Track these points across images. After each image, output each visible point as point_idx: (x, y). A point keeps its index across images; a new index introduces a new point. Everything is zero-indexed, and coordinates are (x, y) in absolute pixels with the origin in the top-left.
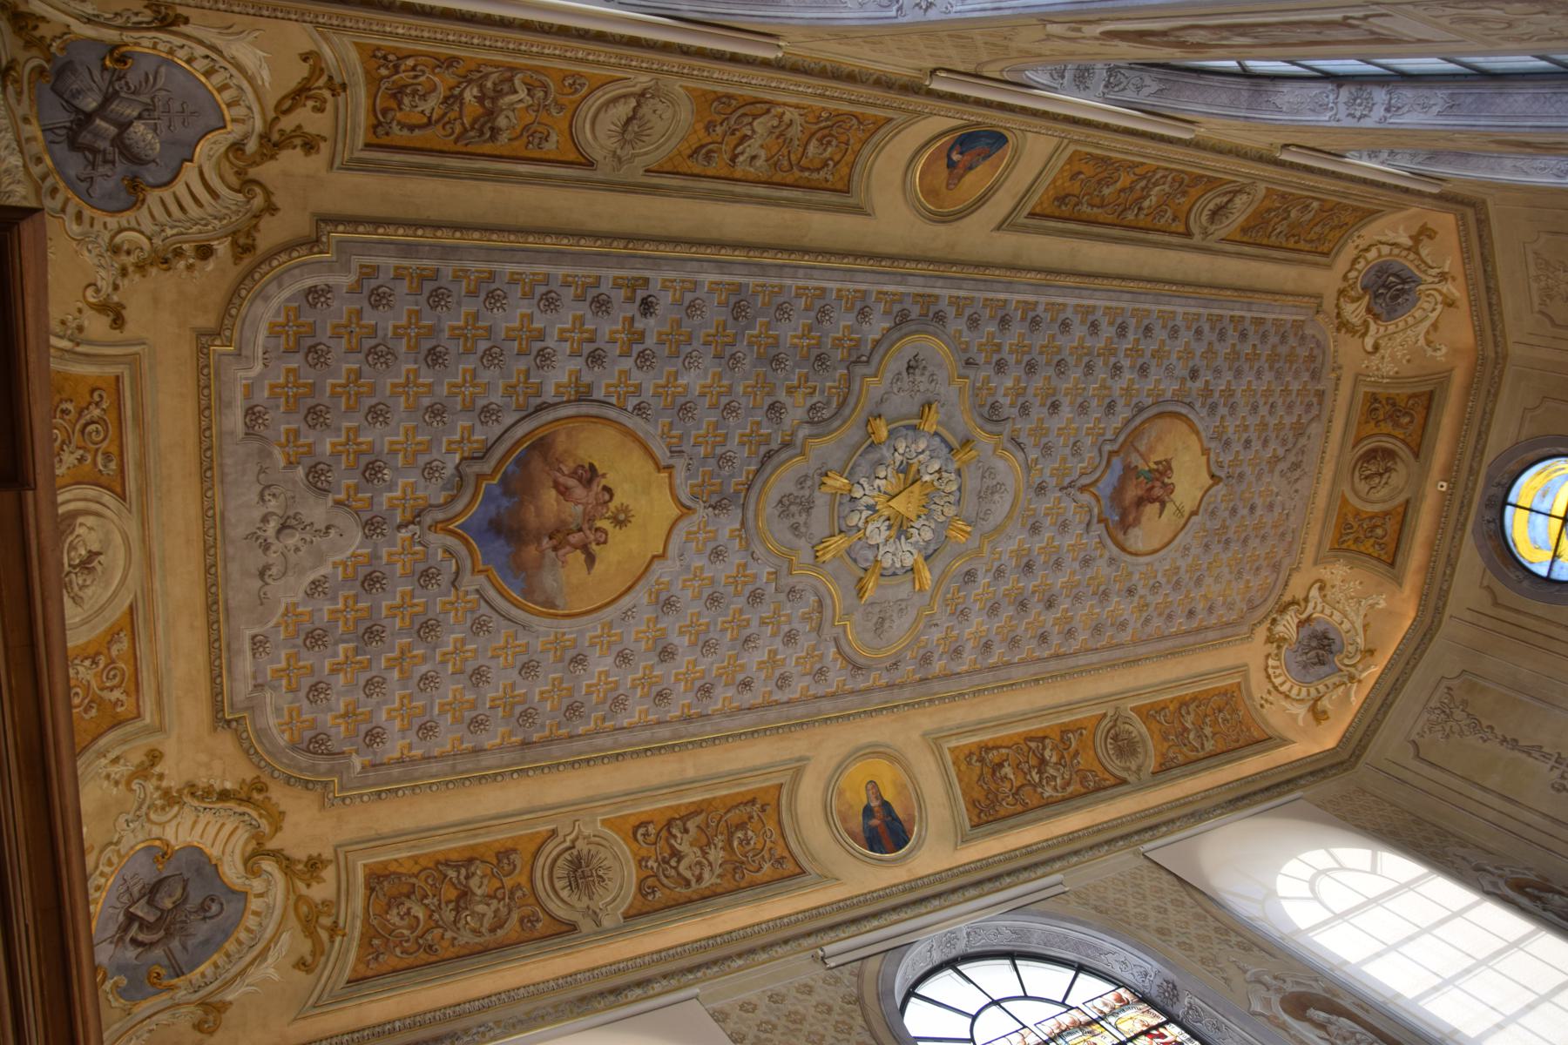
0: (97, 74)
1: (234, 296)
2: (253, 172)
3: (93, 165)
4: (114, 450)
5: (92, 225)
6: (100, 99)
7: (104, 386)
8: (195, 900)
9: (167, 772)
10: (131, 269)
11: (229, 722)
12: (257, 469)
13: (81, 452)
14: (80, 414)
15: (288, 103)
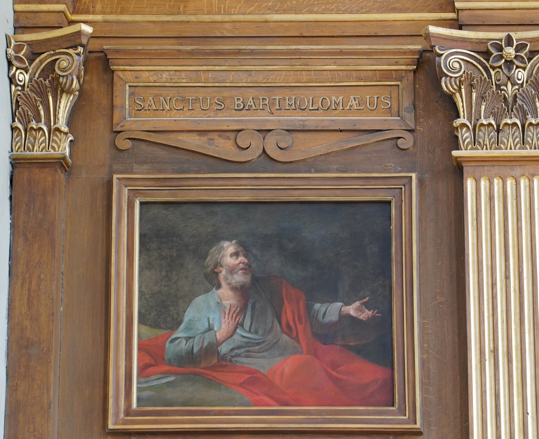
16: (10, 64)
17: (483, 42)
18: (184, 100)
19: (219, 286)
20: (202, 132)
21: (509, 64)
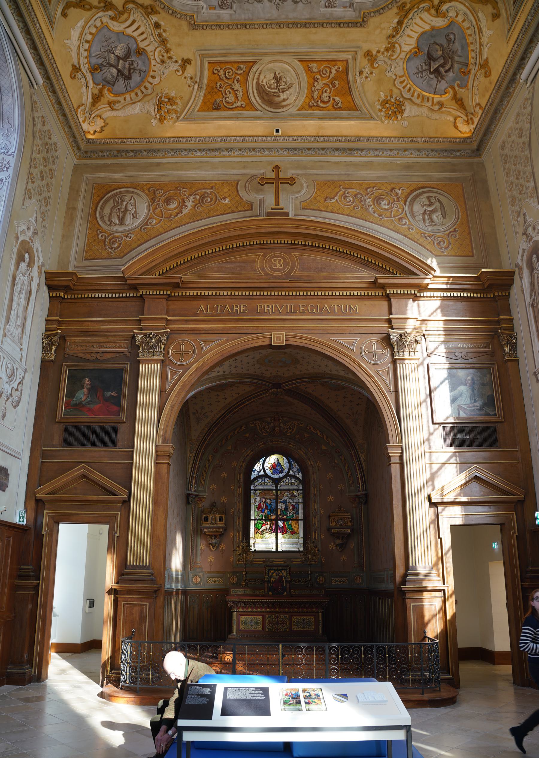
0: (103, 72)
1: (174, 13)
2: (120, 8)
3: (135, 69)
4: (236, 65)
5: (155, 71)
6: (112, 68)
7: (212, 68)
8: (444, 42)
9: (377, 49)
10: (169, 55)
11: (363, 21)
12: (246, 3)
13: (235, 80)
14: (221, 79)
15: (88, 7)
16: (43, 339)
17: (146, 333)
18: (81, 346)
19: (84, 388)
20: (83, 353)
21: (151, 338)
